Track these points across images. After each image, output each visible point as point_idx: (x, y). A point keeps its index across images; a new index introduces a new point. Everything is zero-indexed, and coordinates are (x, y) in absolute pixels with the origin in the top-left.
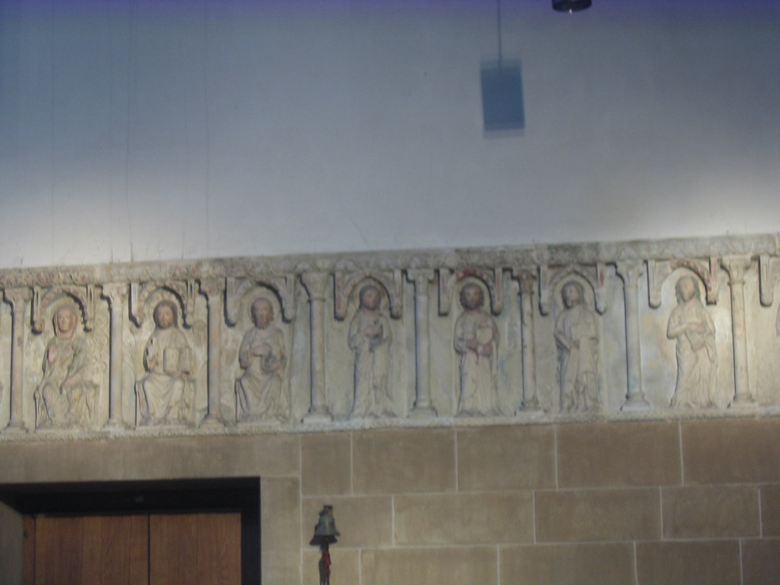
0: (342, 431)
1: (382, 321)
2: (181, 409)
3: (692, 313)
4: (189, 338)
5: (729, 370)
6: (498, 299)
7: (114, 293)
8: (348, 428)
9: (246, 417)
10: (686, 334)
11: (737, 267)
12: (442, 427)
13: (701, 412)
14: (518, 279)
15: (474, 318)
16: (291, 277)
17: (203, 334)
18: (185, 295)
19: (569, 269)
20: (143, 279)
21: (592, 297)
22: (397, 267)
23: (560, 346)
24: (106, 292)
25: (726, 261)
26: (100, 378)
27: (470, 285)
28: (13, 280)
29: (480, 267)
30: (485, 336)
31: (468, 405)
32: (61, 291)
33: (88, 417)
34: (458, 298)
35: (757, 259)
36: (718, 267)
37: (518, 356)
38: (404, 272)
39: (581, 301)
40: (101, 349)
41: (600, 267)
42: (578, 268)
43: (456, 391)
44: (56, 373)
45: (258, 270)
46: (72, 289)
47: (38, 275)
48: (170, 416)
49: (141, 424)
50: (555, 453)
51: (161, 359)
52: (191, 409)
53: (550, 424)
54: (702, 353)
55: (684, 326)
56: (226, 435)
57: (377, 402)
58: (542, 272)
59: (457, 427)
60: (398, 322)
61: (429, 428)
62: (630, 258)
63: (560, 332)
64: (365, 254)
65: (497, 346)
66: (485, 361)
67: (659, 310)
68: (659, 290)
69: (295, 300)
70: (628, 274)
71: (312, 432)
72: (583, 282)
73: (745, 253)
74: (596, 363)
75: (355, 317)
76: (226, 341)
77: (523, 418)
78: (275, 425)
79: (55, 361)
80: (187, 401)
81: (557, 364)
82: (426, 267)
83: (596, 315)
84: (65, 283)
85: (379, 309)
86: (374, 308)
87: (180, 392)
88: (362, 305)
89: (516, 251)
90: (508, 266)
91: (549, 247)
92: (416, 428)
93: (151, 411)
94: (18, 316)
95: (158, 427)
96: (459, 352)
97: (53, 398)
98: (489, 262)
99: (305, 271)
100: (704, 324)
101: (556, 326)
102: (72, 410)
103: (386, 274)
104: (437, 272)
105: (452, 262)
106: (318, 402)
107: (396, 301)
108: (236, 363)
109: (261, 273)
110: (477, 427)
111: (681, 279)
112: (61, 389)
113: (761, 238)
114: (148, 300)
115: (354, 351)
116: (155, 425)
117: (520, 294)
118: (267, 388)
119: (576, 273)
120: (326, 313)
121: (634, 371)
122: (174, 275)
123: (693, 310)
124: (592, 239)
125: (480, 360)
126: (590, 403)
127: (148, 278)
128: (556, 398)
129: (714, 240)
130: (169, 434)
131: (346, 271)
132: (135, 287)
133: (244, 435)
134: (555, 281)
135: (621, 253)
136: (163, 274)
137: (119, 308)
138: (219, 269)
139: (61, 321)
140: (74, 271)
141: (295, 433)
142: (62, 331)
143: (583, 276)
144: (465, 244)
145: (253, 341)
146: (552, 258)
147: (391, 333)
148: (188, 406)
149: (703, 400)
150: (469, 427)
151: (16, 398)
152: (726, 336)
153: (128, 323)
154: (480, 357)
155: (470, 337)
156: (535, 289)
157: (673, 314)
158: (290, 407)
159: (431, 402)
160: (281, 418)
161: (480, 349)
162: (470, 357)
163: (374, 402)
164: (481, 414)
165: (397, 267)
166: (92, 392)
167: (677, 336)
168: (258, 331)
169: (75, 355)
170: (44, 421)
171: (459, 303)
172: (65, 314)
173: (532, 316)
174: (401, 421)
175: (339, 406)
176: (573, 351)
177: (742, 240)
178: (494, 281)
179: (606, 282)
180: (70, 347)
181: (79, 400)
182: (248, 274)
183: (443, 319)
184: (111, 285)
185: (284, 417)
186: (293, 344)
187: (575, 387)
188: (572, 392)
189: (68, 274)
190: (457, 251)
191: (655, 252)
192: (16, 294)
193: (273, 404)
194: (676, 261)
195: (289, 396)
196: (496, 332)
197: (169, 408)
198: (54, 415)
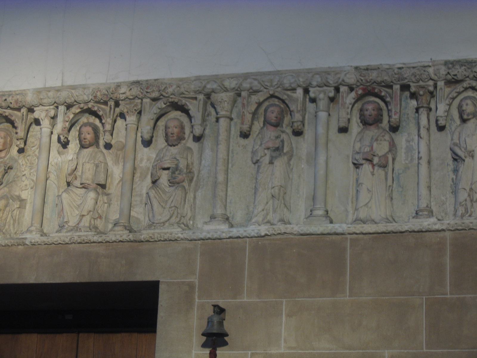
0: (238, 237)
1: (284, 136)
6: (395, 114)
8: (245, 234)
9: (151, 225)
15: (372, 132)
16: (201, 97)
19: (465, 85)
20: (69, 101)
22: (299, 86)
23: (456, 158)
27: (369, 102)
29: (379, 84)
31: (362, 214)
34: (358, 116)
38: (306, 91)
43: (352, 202)
45: (170, 90)
48: (82, 224)
50: (448, 260)
52: (104, 220)
53: (443, 230)
57: (275, 211)
58: (438, 88)
60: (299, 139)
63: (455, 144)
64: (269, 73)
65: (394, 159)
66: (380, 172)
69: (204, 120)
76: (142, 160)
78: (177, 232)
80: (99, 211)
85: (282, 126)
86: (277, 125)
88: (266, 122)
89: (414, 68)
91: (446, 63)
96: (357, 166)
99: (213, 91)
101: (452, 139)
103: (289, 93)
104: (337, 90)
105: (351, 79)
115: (257, 164)
116: (67, 232)
117: (417, 110)
118: (172, 198)
120: (233, 132)
125: (375, 171)
128: (450, 209)
138: (136, 91)
140: (9, 95)
144: (363, 63)
146: (448, 73)
147: (292, 148)
154: (376, 168)
155: (367, 149)
156: (433, 106)
158: (193, 218)
159: (327, 212)
160: (183, 226)
161: (376, 160)
162: (367, 167)
164: (374, 222)
166: (17, 205)
171: (359, 121)
173: (428, 130)
174: (295, 228)
175: (239, 216)
178: (391, 98)
181: (4, 210)
183: (342, 135)
185: (187, 226)
186: (201, 160)
187: (469, 195)
188: (466, 200)
189: (4, 98)
190: (356, 68)
193: (176, 213)
196: (393, 146)
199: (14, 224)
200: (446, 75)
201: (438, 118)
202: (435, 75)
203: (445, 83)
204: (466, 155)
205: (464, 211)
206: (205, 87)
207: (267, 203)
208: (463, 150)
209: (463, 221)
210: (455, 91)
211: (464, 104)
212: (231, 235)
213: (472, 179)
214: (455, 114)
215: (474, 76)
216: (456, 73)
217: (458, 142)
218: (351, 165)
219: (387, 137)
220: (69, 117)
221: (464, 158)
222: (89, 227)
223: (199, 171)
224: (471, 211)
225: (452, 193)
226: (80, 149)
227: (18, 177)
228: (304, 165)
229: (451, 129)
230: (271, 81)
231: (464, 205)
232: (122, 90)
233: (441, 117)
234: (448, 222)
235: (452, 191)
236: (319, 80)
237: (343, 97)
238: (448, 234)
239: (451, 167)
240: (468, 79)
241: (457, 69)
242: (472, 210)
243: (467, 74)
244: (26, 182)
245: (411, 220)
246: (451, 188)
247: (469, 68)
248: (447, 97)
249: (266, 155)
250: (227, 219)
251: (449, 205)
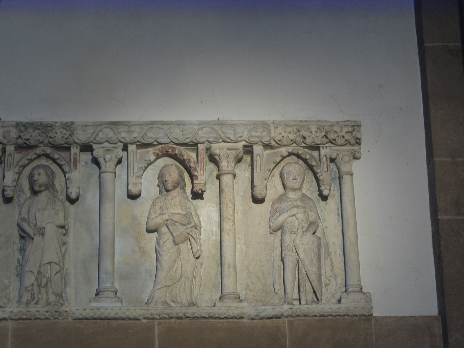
5: (215, 269)
11: (228, 156)
13: (181, 311)
19: (38, 151)
21: (63, 184)
23: (24, 236)
25: (216, 148)
35: (249, 150)
36: (206, 159)
39: (50, 186)
41: (75, 150)
42: (49, 151)
54: (184, 247)
55: (166, 217)
58: (7, 153)
63: (24, 220)
68: (140, 177)
72: (54, 167)
74: (64, 256)
81: (18, 255)
83: (67, 204)
91: (18, 125)
100: (188, 216)
101: (20, 214)
111: (165, 166)
113: (255, 125)
119: (47, 156)
121: (106, 264)
123: (177, 200)
126: (52, 298)
128: (14, 294)
129: (202, 124)
135: (97, 135)
143: (54, 161)
146: (20, 136)
149: (184, 299)
152: (212, 232)
157: (154, 204)
176: (37, 238)
177: (233, 126)
179: (80, 165)
187: (37, 279)
188: (33, 285)
191: (137, 134)
200: (17, 139)
201: (5, 188)
202: (5, 138)
203: (15, 147)
204: (36, 232)
205: (30, 298)
208: (32, 226)
209: (29, 309)
210: (26, 157)
211: (36, 173)
213: (41, 260)
214: (25, 184)
215: (49, 142)
216: (28, 137)
217: (27, 217)
221: (33, 236)
224: (38, 297)
225: (17, 275)
229: (19, 201)
231: (31, 291)
233: (9, 187)
234: (11, 310)
235: (16, 273)
238: (10, 324)
239: (17, 246)
240: (42, 145)
241: (30, 132)
242: (40, 296)
243: (41, 139)
246: (16, 269)
247: (43, 133)
248: (17, 165)
251: (13, 289)
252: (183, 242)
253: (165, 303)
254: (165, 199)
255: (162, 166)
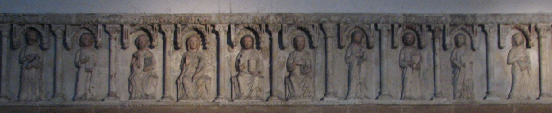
0: (344, 105)
1: (363, 50)
2: (257, 91)
3: (521, 51)
4: (259, 55)
6: (424, 41)
7: (221, 29)
8: (347, 104)
9: (294, 97)
10: (518, 62)
12: (395, 105)
13: (526, 102)
14: (433, 32)
16: (316, 25)
17: (267, 53)
18: (260, 32)
19: (460, 27)
21: (470, 42)
22: (372, 22)
23: (454, 66)
24: (217, 29)
25: (539, 26)
26: (212, 74)
28: (166, 21)
29: (414, 24)
30: (417, 59)
31: (408, 94)
32: (192, 27)
33: (206, 94)
37: (431, 71)
38: (376, 26)
40: (212, 59)
42: (464, 27)
44: (189, 71)
45: (299, 20)
46: (199, 26)
47: (181, 18)
49: (236, 99)
51: (246, 65)
53: (450, 105)
54: (525, 72)
55: (517, 58)
56: (282, 106)
57: (361, 91)
59: (403, 105)
60: (371, 50)
61: (389, 105)
62: (491, 23)
64: (357, 14)
66: (416, 72)
67: (503, 50)
68: (505, 40)
70: (489, 31)
71: (328, 105)
73: (548, 23)
75: (348, 47)
76: (279, 57)
77: (435, 101)
78: (309, 101)
79: (189, 64)
81: (452, 75)
82: (387, 23)
84: (195, 23)
86: (359, 43)
87: (257, 82)
88: (353, 41)
90: (430, 24)
91: (452, 16)
92: (382, 105)
93: (242, 92)
94: (168, 40)
95: (246, 101)
96: (402, 67)
97: (188, 83)
98: (420, 21)
99: (324, 22)
101: (451, 56)
102: (199, 90)
104: (393, 26)
105: (401, 20)
106: (330, 90)
107: (371, 40)
108: (285, 69)
109: (301, 22)
110: (413, 105)
112: (192, 78)
114: (239, 34)
116: (244, 99)
117: (433, 39)
118: (304, 83)
119: (463, 29)
121: (492, 80)
122: (255, 21)
124: (472, 12)
127: (240, 22)
130: (252, 104)
131: (346, 23)
132: (233, 26)
133: (292, 106)
134: (453, 33)
136: (249, 21)
137: (223, 38)
138: (279, 19)
139: (192, 43)
140: (200, 17)
141: (319, 106)
142: (192, 49)
143: (466, 31)
144: (408, 12)
145: (295, 58)
146: (452, 21)
148: (260, 90)
150: (409, 105)
151: (167, 83)
153: (227, 46)
154: (414, 71)
158: (314, 92)
161: (415, 66)
162: (409, 70)
163: (359, 91)
165: (372, 22)
167: (513, 64)
168: (298, 52)
169: (199, 61)
170: (183, 96)
171: (402, 42)
172: (194, 39)
176: (462, 69)
178: (421, 31)
179: (478, 34)
180: (196, 57)
182: (294, 22)
183: (393, 50)
184: (220, 25)
188: (461, 89)
189: (197, 18)
190: (404, 15)
191: (504, 20)
192: (168, 27)
194: (514, 25)
195: (314, 86)
197: (251, 91)
198: (189, 93)
199: (207, 93)
206: (320, 19)
207: (357, 87)
212: (340, 104)
216: (456, 21)
218: (398, 67)
219: (418, 53)
220: (237, 31)
222: (256, 96)
223: (315, 66)
226: (242, 49)
227: (206, 64)
228: (373, 66)
230: (358, 19)
232: (272, 18)
236: (384, 20)
237: (396, 29)
244: (210, 67)
245: (434, 99)
249: (355, 60)
250: (335, 94)
252: (525, 70)
253: (518, 98)
254: (516, 50)
255: (513, 34)
